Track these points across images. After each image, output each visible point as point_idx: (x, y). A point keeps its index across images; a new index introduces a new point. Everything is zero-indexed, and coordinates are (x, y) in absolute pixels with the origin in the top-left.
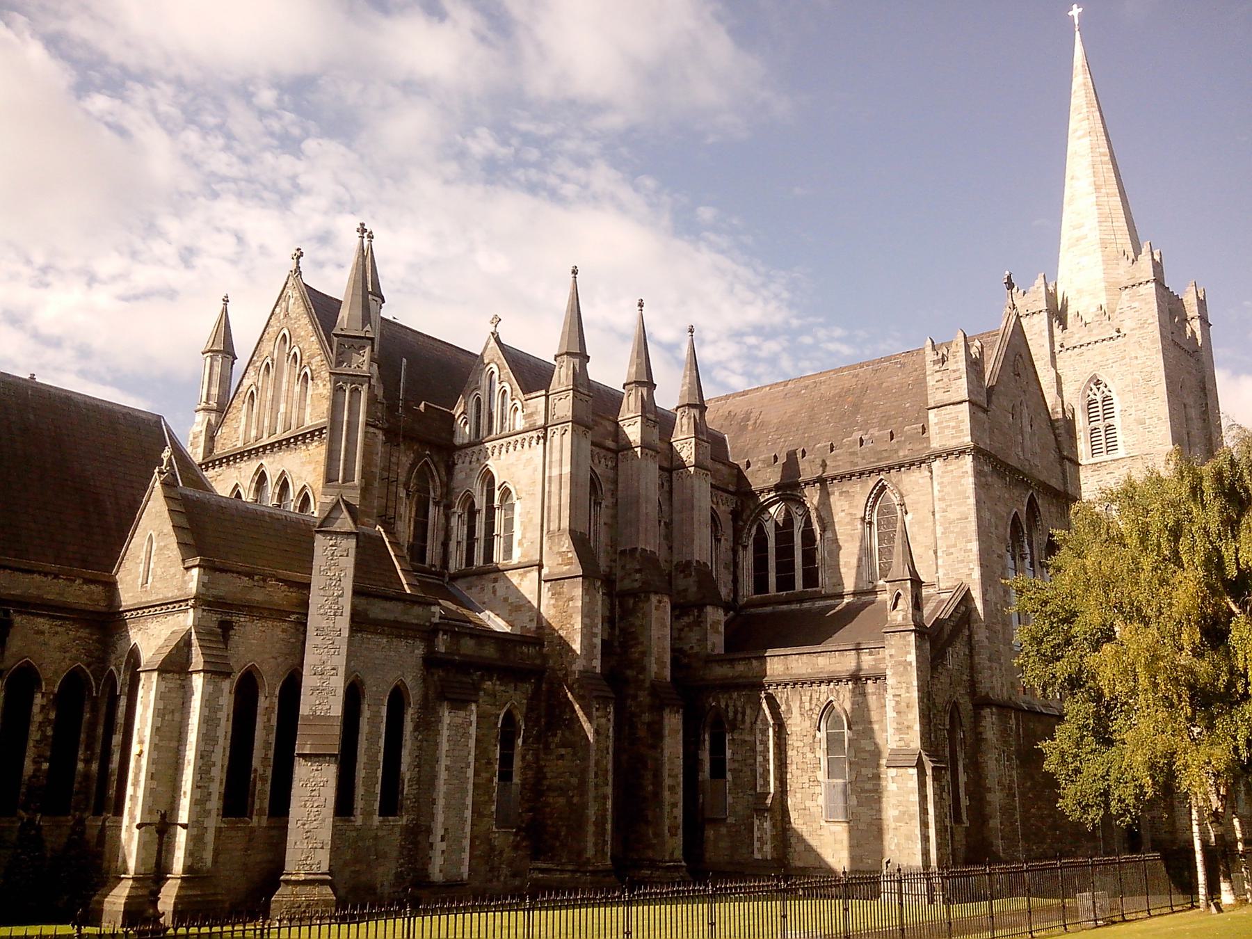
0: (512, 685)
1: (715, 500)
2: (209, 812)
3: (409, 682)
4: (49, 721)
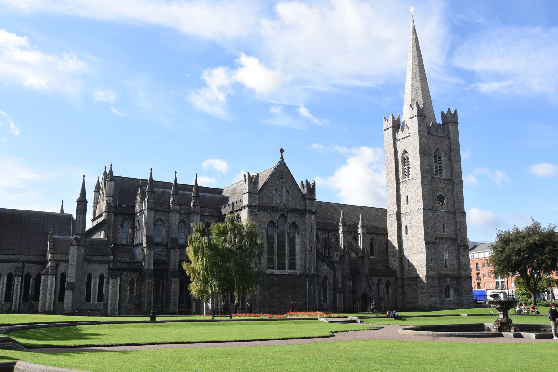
0: (133, 273)
1: (210, 219)
2: (52, 301)
3: (104, 273)
4: (34, 284)
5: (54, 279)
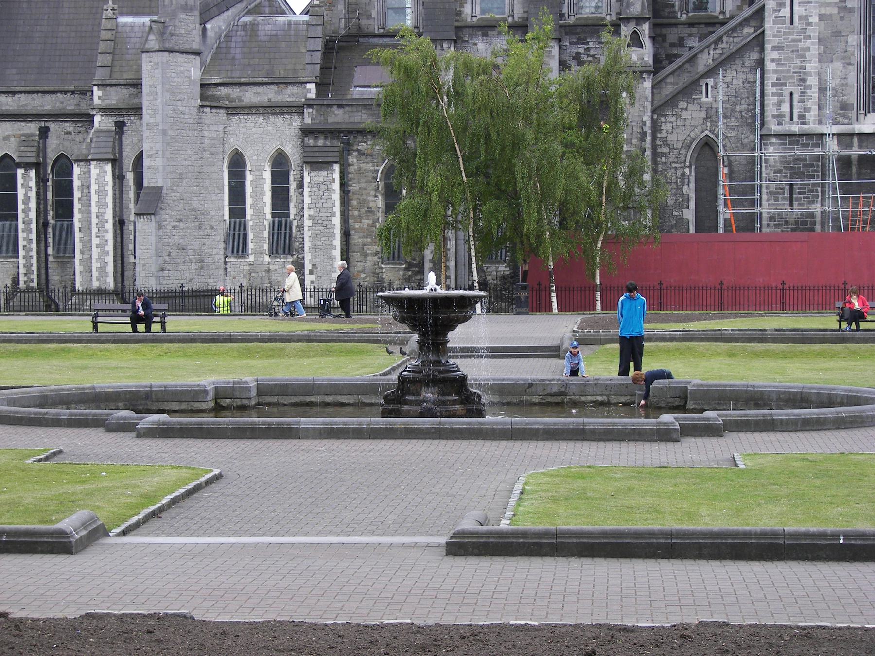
2: (108, 252)
5: (109, 178)
